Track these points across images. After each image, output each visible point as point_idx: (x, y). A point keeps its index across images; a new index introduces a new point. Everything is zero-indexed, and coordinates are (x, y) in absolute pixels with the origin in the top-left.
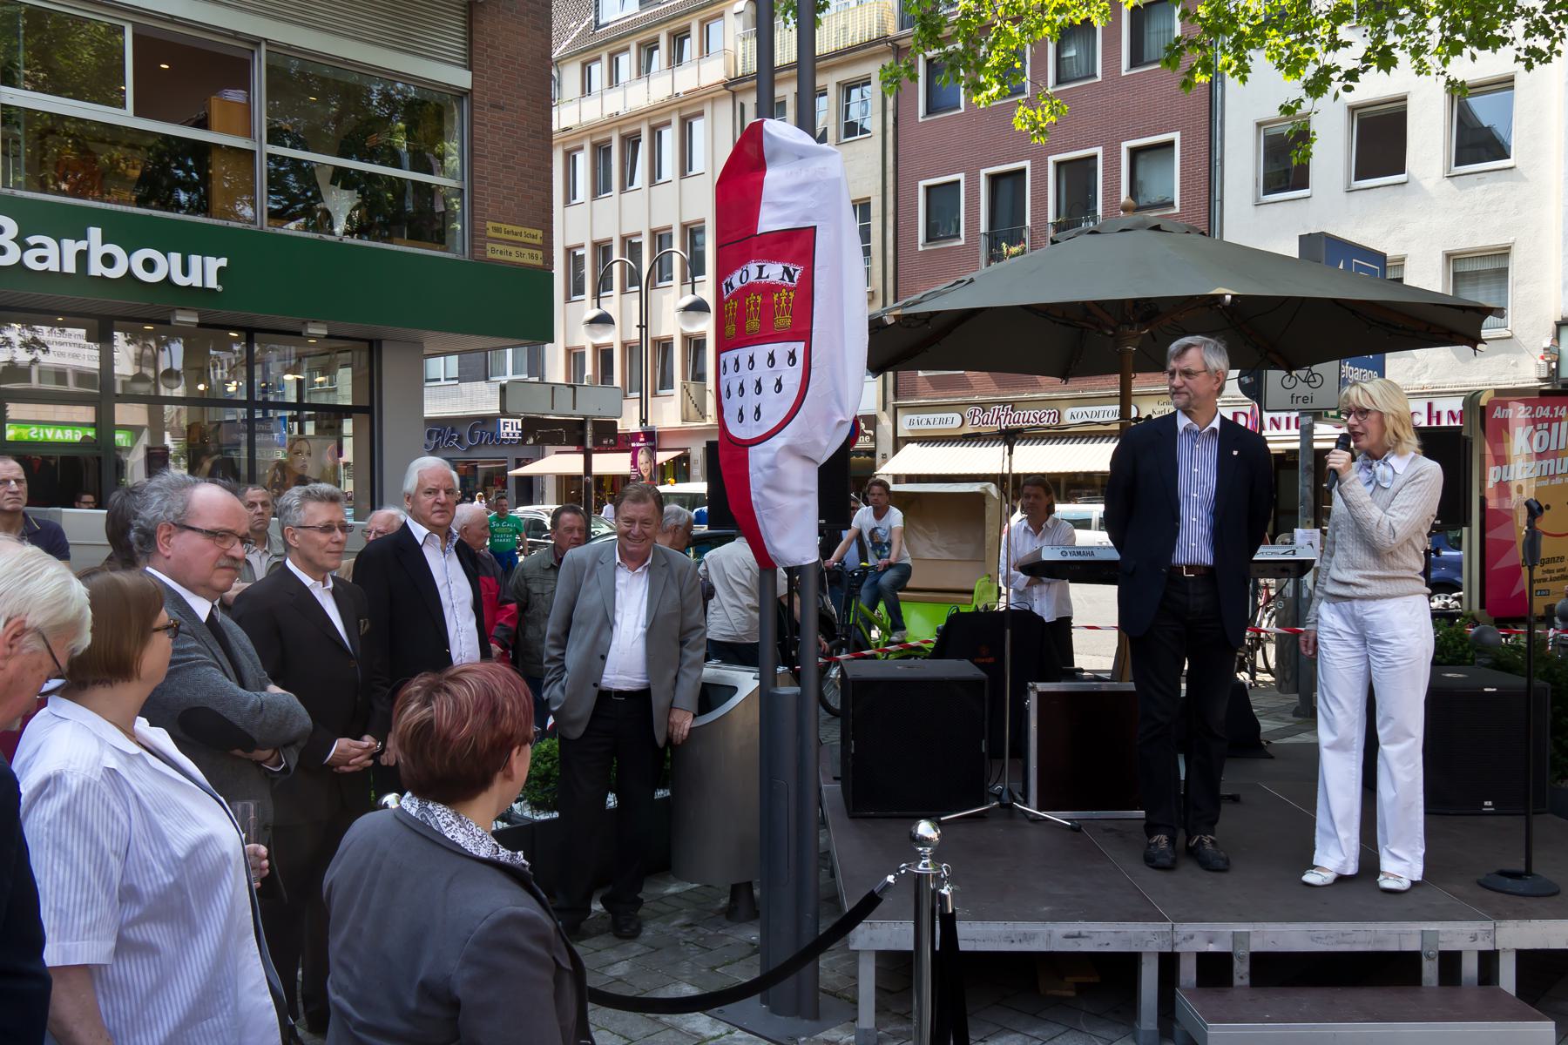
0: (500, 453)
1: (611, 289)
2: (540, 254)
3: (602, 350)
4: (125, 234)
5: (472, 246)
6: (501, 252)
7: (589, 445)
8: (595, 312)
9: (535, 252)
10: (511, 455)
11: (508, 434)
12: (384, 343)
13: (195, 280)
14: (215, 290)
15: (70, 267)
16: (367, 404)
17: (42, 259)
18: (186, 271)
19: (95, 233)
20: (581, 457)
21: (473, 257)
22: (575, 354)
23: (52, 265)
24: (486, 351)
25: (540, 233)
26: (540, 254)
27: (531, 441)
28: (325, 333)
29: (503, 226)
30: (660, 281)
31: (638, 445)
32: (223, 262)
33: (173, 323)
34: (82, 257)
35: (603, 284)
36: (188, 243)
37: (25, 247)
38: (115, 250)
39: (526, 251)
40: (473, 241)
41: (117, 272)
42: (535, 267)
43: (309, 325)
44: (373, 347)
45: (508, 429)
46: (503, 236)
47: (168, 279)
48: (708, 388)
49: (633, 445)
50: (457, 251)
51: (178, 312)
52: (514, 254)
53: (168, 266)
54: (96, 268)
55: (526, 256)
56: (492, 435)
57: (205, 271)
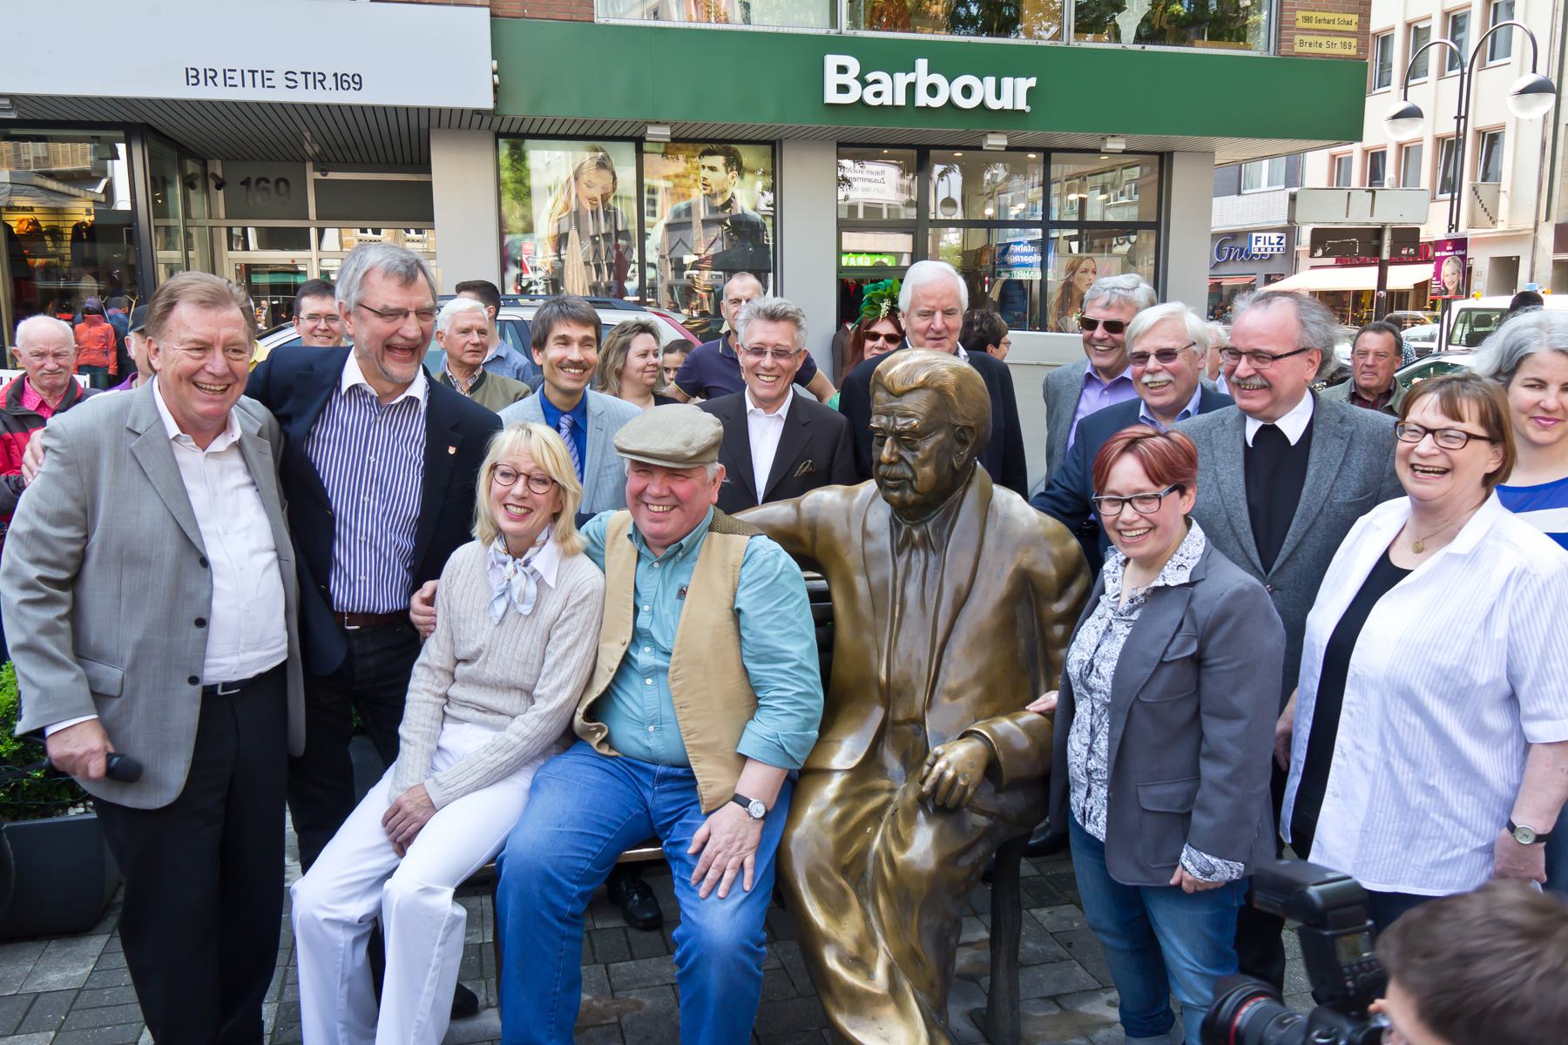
0: (1250, 268)
1: (1389, 85)
2: (1354, 42)
3: (1372, 154)
4: (948, 63)
5: (1279, 41)
6: (1310, 44)
7: (1386, 255)
8: (1402, 106)
9: (1348, 40)
10: (1261, 270)
11: (1260, 249)
12: (1175, 154)
13: (1006, 103)
14: (1023, 111)
15: (901, 100)
16: (1154, 220)
17: (878, 94)
18: (998, 96)
19: (922, 64)
20: (1375, 270)
21: (1279, 52)
22: (1340, 160)
23: (886, 100)
24: (1239, 165)
25: (1355, 18)
26: (1354, 42)
27: (1320, 252)
28: (1123, 147)
29: (1314, 15)
30: (1492, 59)
31: (1444, 254)
32: (1032, 82)
33: (984, 148)
34: (911, 88)
35: (1414, 71)
36: (999, 66)
37: (865, 84)
38: (939, 79)
39: (1337, 40)
40: (1280, 34)
41: (938, 102)
42: (1347, 58)
43: (1108, 140)
44: (1164, 159)
45: (1260, 244)
46: (1313, 25)
47: (982, 104)
48: (1502, 189)
49: (1438, 254)
50: (1259, 47)
51: (989, 136)
52: (1324, 45)
53: (984, 90)
54: (922, 99)
55: (1339, 45)
56: (1242, 250)
57: (1015, 93)
